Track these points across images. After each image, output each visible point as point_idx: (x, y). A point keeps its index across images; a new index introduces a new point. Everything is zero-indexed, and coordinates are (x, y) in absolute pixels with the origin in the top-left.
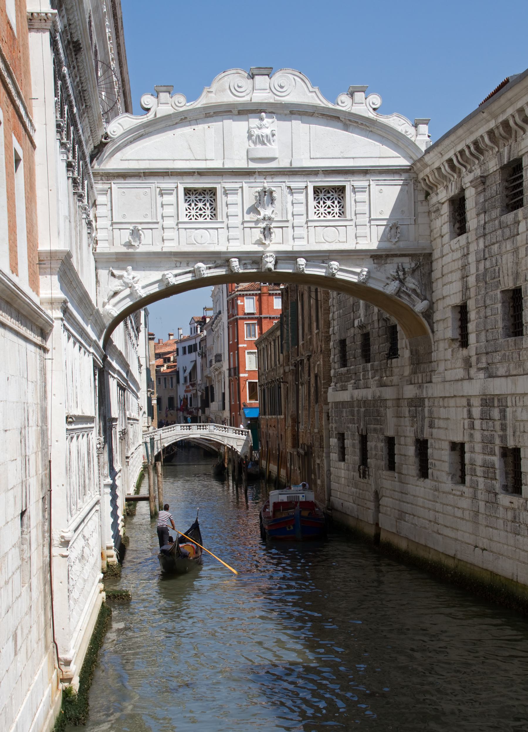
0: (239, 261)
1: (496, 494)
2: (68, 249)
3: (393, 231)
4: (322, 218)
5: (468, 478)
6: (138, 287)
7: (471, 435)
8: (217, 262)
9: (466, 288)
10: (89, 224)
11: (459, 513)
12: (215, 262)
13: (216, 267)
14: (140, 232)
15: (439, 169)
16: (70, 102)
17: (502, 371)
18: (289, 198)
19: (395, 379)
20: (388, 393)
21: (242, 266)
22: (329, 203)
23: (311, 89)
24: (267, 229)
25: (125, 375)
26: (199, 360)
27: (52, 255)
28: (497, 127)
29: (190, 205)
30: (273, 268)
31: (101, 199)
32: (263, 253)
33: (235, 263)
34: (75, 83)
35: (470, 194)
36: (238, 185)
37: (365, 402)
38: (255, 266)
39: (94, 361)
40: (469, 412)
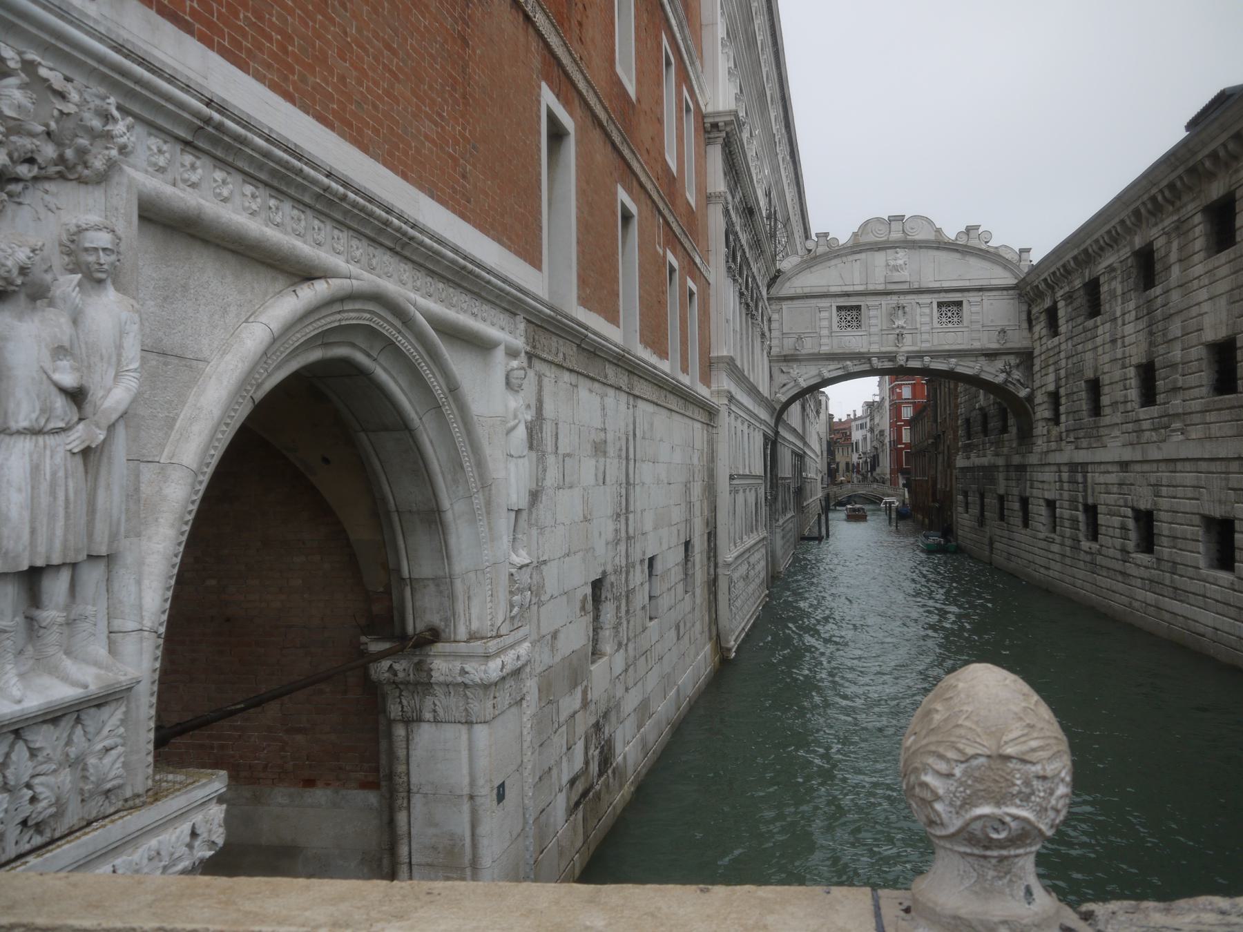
0: (879, 358)
1: (1079, 541)
2: (732, 354)
3: (1002, 334)
5: (1058, 528)
6: (801, 380)
7: (1061, 494)
9: (1058, 379)
10: (763, 335)
11: (1050, 556)
15: (1037, 286)
16: (743, 250)
17: (1085, 445)
18: (918, 310)
19: (1005, 450)
20: (1000, 461)
22: (949, 314)
25: (800, 445)
26: (869, 435)
27: (720, 359)
28: (1079, 254)
31: (775, 316)
32: (897, 353)
33: (875, 360)
35: (1061, 304)
36: (877, 303)
37: (982, 468)
40: (1060, 476)
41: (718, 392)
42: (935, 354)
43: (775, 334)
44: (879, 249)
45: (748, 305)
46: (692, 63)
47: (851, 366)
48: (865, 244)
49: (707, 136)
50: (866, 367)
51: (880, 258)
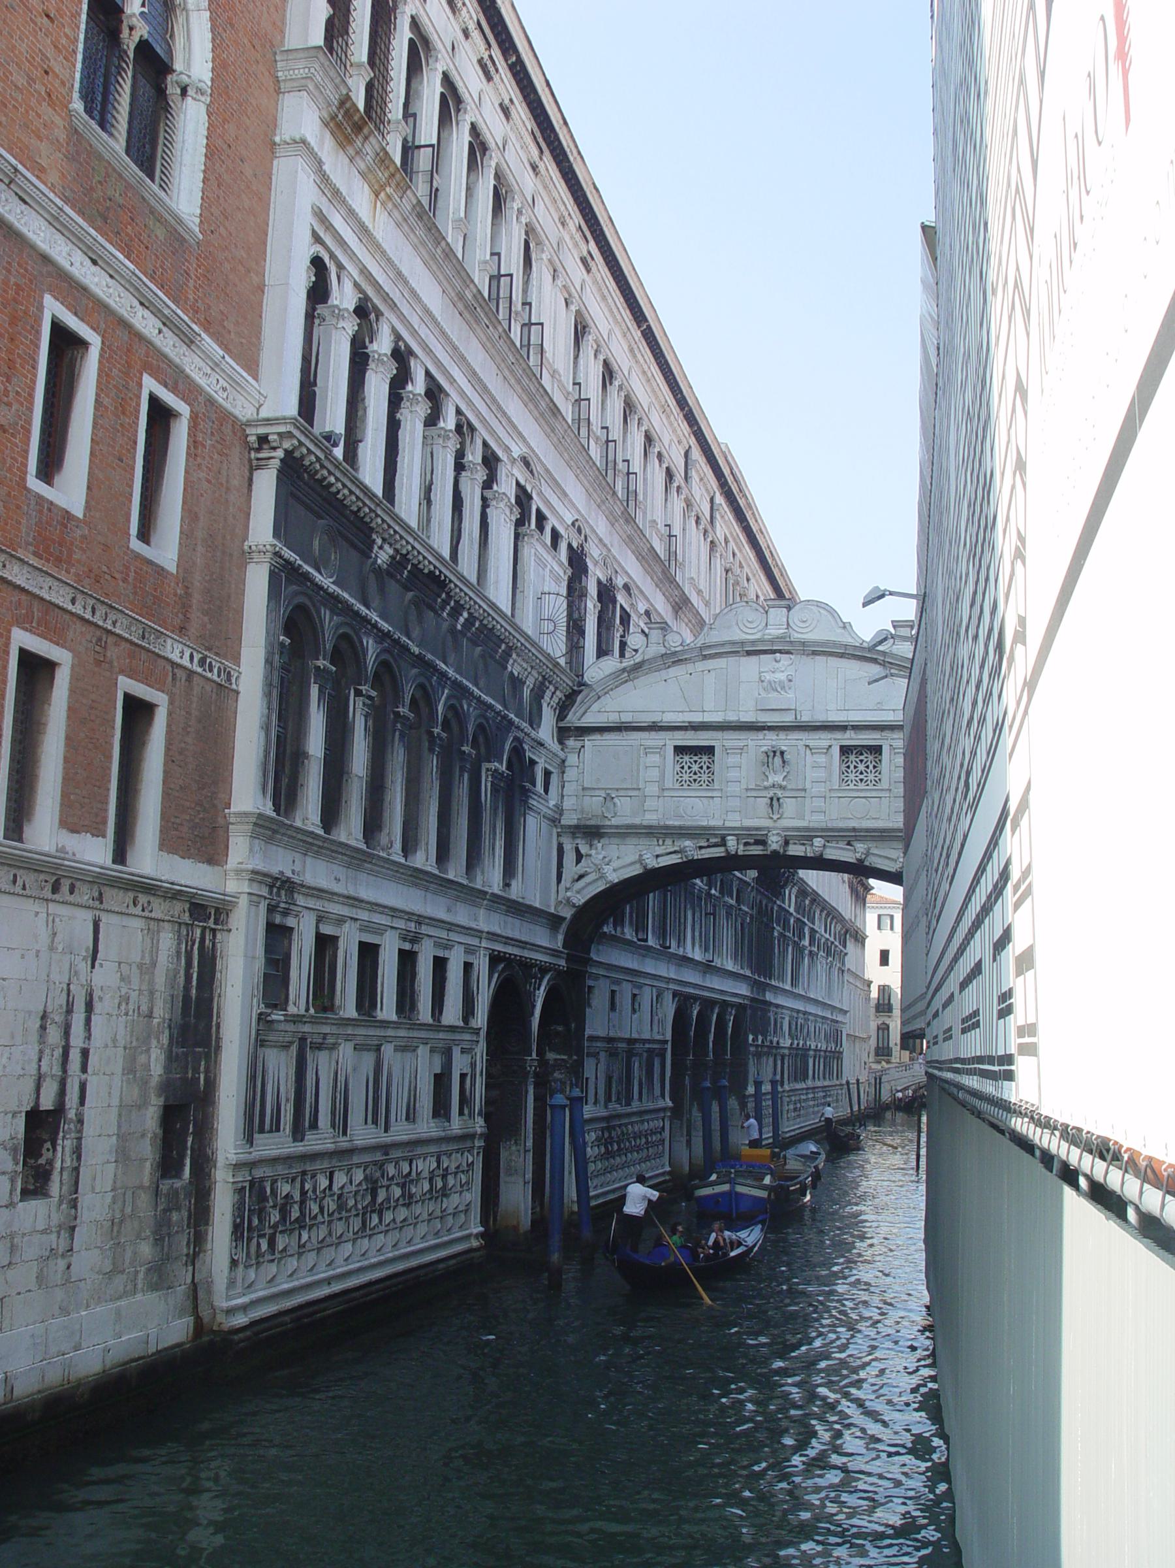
0: (738, 840)
4: (852, 787)
8: (711, 840)
12: (708, 840)
13: (709, 847)
14: (616, 800)
16: (397, 642)
21: (741, 847)
22: (861, 767)
23: (842, 625)
24: (775, 799)
25: (743, 990)
29: (683, 768)
30: (782, 851)
31: (572, 759)
32: (769, 829)
33: (731, 842)
34: (462, 620)
38: (761, 847)
39: (495, 959)
41: (238, 872)
42: (832, 835)
43: (569, 789)
44: (749, 653)
45: (430, 734)
46: (190, 341)
47: (692, 850)
48: (723, 645)
49: (253, 455)
50: (718, 852)
51: (750, 667)
